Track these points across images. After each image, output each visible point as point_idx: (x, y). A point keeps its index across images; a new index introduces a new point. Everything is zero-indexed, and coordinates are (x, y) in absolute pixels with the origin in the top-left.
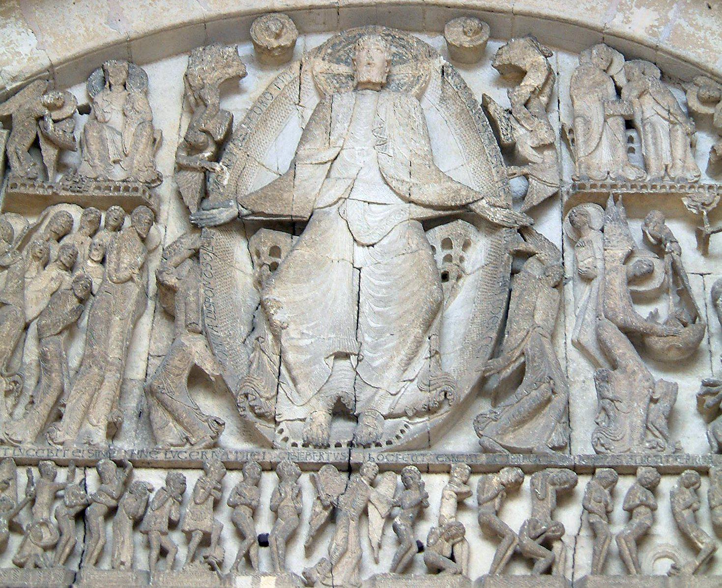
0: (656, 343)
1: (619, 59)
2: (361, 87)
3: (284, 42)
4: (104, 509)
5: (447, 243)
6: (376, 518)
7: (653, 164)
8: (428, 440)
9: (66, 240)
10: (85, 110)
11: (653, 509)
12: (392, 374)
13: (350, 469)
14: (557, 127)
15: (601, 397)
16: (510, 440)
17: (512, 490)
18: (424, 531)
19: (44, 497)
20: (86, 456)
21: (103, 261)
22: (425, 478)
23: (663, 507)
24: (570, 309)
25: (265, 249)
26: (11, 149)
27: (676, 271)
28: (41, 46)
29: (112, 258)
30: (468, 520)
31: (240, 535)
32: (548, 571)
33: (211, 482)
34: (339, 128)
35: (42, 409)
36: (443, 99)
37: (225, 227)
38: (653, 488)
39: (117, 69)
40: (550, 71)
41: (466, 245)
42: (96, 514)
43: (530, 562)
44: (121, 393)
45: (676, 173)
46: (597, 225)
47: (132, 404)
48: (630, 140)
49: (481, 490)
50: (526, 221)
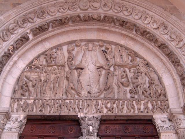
0: (124, 84)
1: (120, 47)
2: (89, 50)
3: (79, 44)
4: (62, 105)
6: (93, 106)
7: (124, 61)
8: (99, 96)
10: (56, 53)
11: (124, 105)
13: (90, 100)
14: (112, 55)
15: (118, 91)
16: (108, 96)
17: (108, 102)
18: (99, 107)
19: (56, 104)
20: (60, 99)
21: (60, 73)
22: (98, 101)
23: (125, 104)
24: (114, 79)
25: (79, 72)
26: (47, 59)
27: (127, 75)
28: (50, 45)
29: (61, 73)
30: (104, 106)
31: (78, 108)
32: (113, 112)
33: (74, 102)
34: (87, 56)
36: (99, 52)
37: (74, 69)
38: (124, 102)
40: (112, 48)
41: (102, 71)
42: (62, 106)
43: (111, 111)
44: (63, 90)
45: (127, 62)
46: (117, 69)
47: (64, 91)
48: (121, 57)
49: (105, 103)
50: (109, 69)
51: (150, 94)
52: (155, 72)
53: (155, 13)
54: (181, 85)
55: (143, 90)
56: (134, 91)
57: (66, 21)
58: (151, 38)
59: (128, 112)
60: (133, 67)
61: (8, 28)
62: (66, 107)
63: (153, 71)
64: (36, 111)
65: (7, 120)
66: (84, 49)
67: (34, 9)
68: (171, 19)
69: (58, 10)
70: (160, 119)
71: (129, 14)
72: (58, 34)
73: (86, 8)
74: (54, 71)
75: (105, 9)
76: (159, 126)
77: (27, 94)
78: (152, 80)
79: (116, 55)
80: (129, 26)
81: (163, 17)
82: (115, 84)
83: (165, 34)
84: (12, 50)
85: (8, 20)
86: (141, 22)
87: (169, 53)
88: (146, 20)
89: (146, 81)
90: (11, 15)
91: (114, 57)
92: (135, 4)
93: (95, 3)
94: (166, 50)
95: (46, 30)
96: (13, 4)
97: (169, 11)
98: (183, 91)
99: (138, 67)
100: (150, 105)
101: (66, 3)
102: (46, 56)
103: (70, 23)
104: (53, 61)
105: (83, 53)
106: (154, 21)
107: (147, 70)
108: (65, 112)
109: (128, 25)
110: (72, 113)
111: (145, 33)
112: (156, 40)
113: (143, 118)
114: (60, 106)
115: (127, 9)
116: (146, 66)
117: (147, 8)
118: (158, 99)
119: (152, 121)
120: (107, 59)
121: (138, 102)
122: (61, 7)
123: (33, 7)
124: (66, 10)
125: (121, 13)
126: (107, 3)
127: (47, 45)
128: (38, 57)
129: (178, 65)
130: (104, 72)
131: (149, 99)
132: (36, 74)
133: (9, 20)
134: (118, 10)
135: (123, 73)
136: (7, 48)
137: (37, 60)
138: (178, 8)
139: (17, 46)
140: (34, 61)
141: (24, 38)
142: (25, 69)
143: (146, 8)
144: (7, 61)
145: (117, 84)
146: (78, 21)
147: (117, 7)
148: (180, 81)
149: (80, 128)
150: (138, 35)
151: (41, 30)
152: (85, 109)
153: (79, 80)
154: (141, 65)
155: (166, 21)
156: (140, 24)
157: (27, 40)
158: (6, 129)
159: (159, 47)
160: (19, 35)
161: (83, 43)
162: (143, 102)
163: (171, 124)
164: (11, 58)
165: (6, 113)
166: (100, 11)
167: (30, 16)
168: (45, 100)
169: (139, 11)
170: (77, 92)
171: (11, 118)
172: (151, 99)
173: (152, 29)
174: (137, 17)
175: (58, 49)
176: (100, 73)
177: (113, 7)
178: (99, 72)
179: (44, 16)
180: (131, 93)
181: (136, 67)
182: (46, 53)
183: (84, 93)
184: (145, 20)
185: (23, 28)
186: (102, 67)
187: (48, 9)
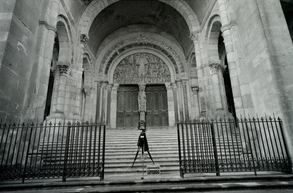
64: (122, 83)
70: (167, 84)
72: (129, 51)
100: (164, 80)
108: (133, 83)
110: (136, 83)
111: (163, 51)
121: (160, 78)
127: (125, 56)
130: (147, 66)
151: (122, 50)
153: (138, 70)
166: (145, 41)
183: (140, 75)
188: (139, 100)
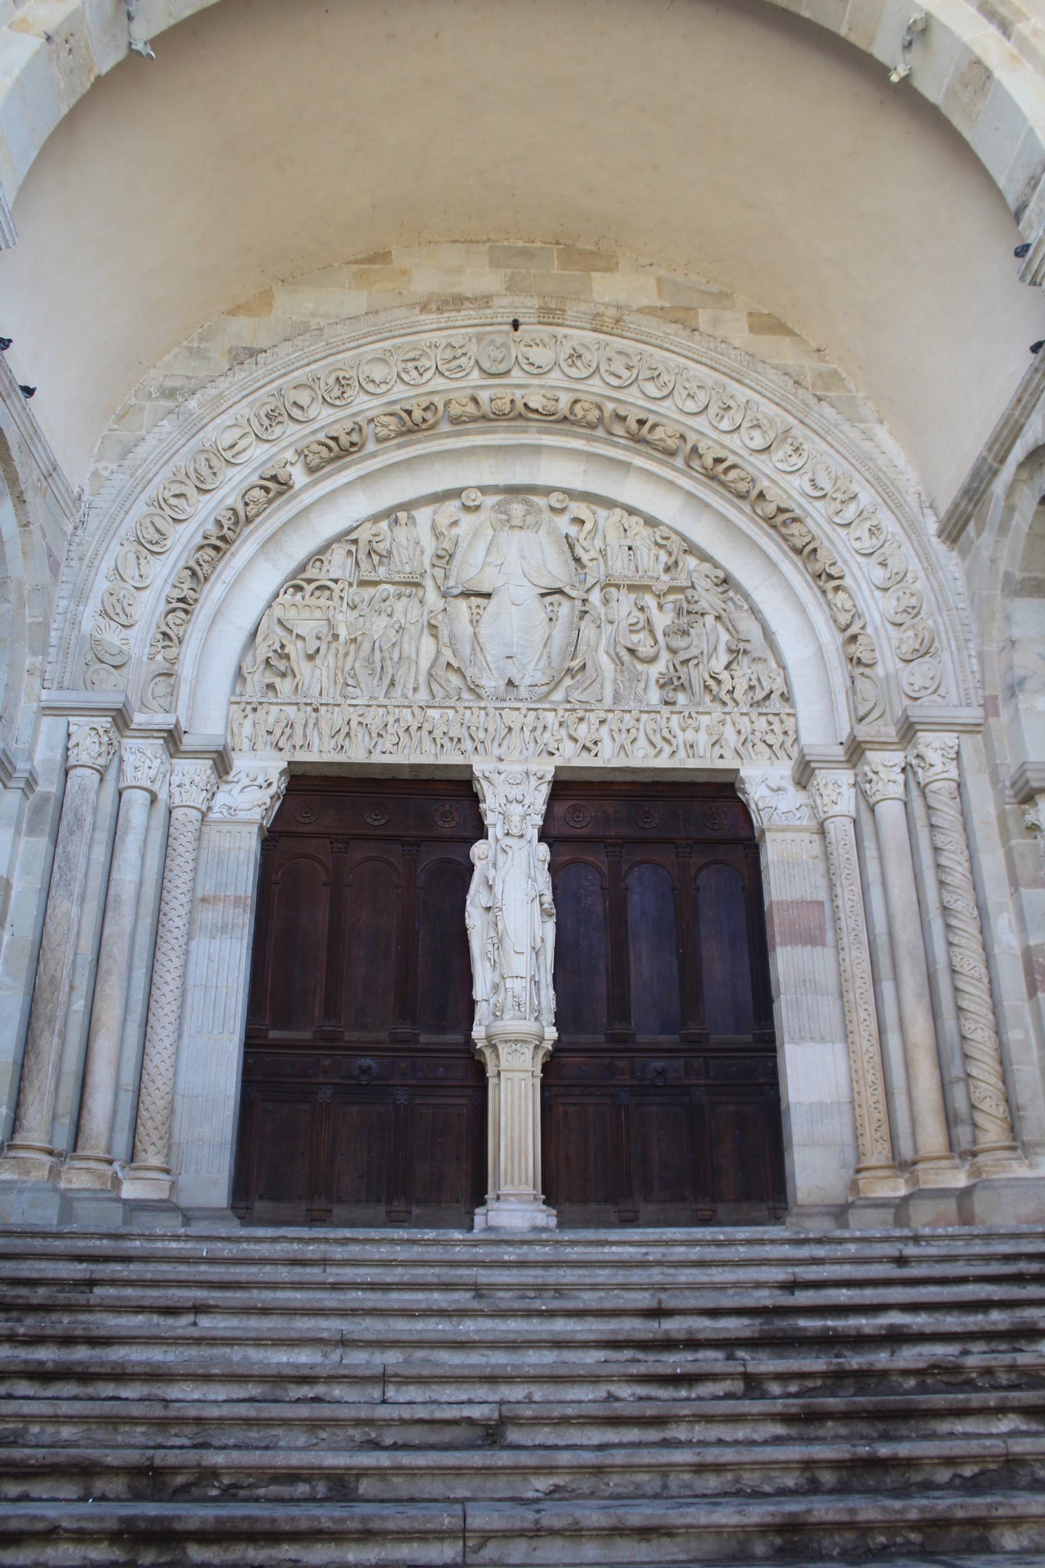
1: (626, 514)
3: (476, 503)
5: (551, 604)
9: (387, 603)
12: (531, 667)
17: (581, 719)
24: (603, 635)
25: (474, 607)
32: (596, 755)
35: (386, 682)
38: (638, 720)
39: (402, 515)
41: (560, 604)
45: (650, 574)
50: (585, 596)
51: (733, 691)
52: (754, 611)
53: (759, 393)
54: (843, 658)
55: (707, 677)
56: (675, 680)
57: (429, 415)
58: (742, 487)
59: (653, 755)
60: (672, 590)
61: (215, 443)
62: (430, 732)
63: (746, 607)
65: (220, 777)
66: (494, 522)
67: (308, 369)
68: (816, 415)
69: (399, 376)
71: (660, 395)
73: (503, 368)
74: (384, 601)
75: (573, 372)
76: (761, 806)
77: (285, 686)
78: (740, 640)
79: (612, 549)
80: (661, 440)
81: (789, 407)
82: (607, 653)
83: (790, 473)
84: (232, 527)
85: (215, 413)
86: (706, 423)
87: (808, 544)
88: (726, 418)
89: (717, 641)
90: (227, 392)
91: (603, 552)
92: (685, 357)
93: (535, 348)
94: (796, 533)
95: (355, 449)
96: (230, 351)
97: (813, 386)
98: (849, 684)
99: (691, 590)
100: (729, 733)
101: (430, 347)
102: (353, 548)
103: (445, 427)
104: (380, 563)
105: (489, 538)
106: (755, 423)
107: (723, 605)
109: (657, 437)
112: (761, 495)
113: (703, 778)
114: (407, 729)
115: (656, 373)
116: (721, 589)
117: (729, 372)
118: (760, 710)
119: (737, 786)
120: (577, 560)
122: (410, 365)
123: (306, 361)
124: (428, 375)
125: (634, 389)
126: (581, 350)
128: (326, 547)
129: (837, 589)
131: (727, 710)
132: (318, 614)
133: (219, 411)
134: (620, 377)
135: (639, 614)
136: (212, 519)
137: (321, 561)
138: (844, 374)
139: (249, 508)
140: (311, 563)
141: (274, 478)
142: (278, 596)
143: (724, 374)
144: (213, 564)
145: (614, 656)
146: (474, 419)
147: (619, 367)
148: (840, 649)
149: (478, 807)
150: (698, 476)
152: (496, 744)
154: (702, 583)
155: (800, 426)
156: (701, 433)
157: (285, 487)
158: (216, 810)
159: (769, 520)
160: (254, 471)
161: (491, 500)
162: (705, 720)
163: (803, 802)
164: (228, 555)
165: (214, 756)
167: (293, 396)
168: (351, 709)
169: (700, 384)
170: (469, 679)
171: (232, 773)
172: (736, 709)
173: (745, 453)
174: (690, 406)
175: (396, 521)
176: (552, 611)
177: (603, 368)
178: (549, 609)
179: (345, 395)
180: (662, 687)
181: (680, 589)
182: (352, 536)
184: (722, 417)
185: (268, 441)
186: (560, 592)
187: (361, 370)
188: (474, 918)
